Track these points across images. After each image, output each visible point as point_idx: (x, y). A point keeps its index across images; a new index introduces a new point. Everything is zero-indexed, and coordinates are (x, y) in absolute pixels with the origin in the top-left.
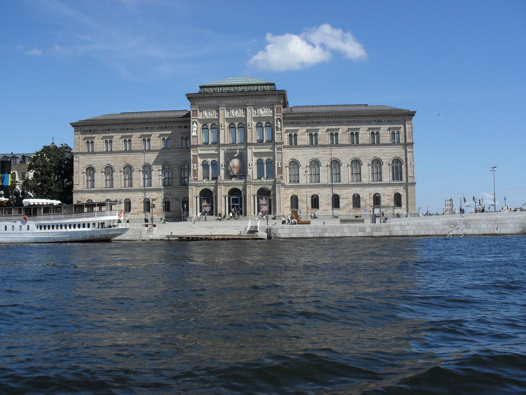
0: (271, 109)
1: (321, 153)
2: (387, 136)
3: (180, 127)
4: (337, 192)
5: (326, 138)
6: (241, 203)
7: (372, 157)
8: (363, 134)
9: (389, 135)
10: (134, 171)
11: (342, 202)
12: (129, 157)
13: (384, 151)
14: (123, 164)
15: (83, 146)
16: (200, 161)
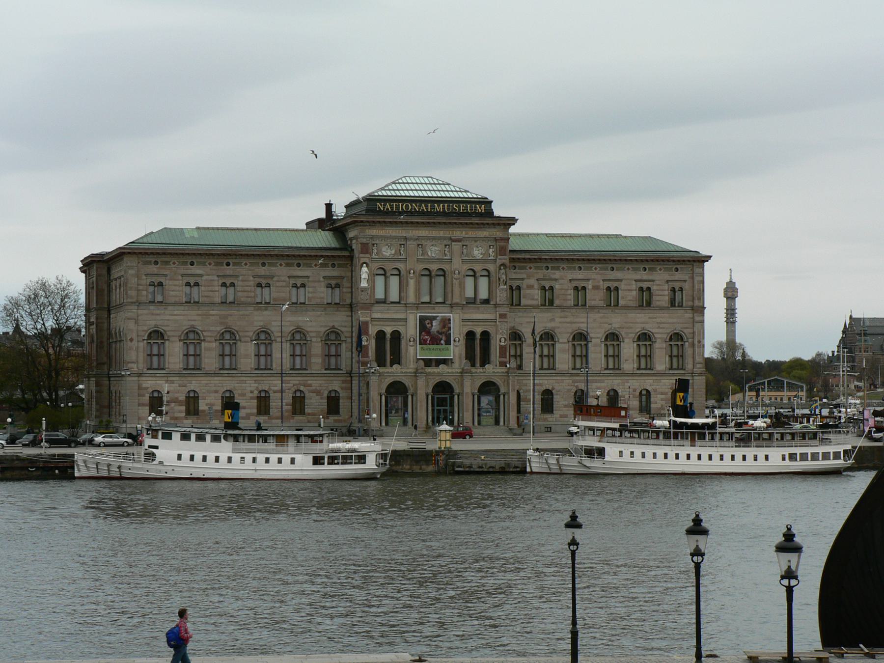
0: (490, 246)
1: (558, 320)
2: (664, 295)
5: (566, 295)
6: (452, 405)
7: (638, 329)
8: (624, 290)
9: (666, 293)
10: (240, 340)
12: (231, 316)
13: (658, 320)
14: (218, 329)
15: (143, 290)
16: (373, 330)
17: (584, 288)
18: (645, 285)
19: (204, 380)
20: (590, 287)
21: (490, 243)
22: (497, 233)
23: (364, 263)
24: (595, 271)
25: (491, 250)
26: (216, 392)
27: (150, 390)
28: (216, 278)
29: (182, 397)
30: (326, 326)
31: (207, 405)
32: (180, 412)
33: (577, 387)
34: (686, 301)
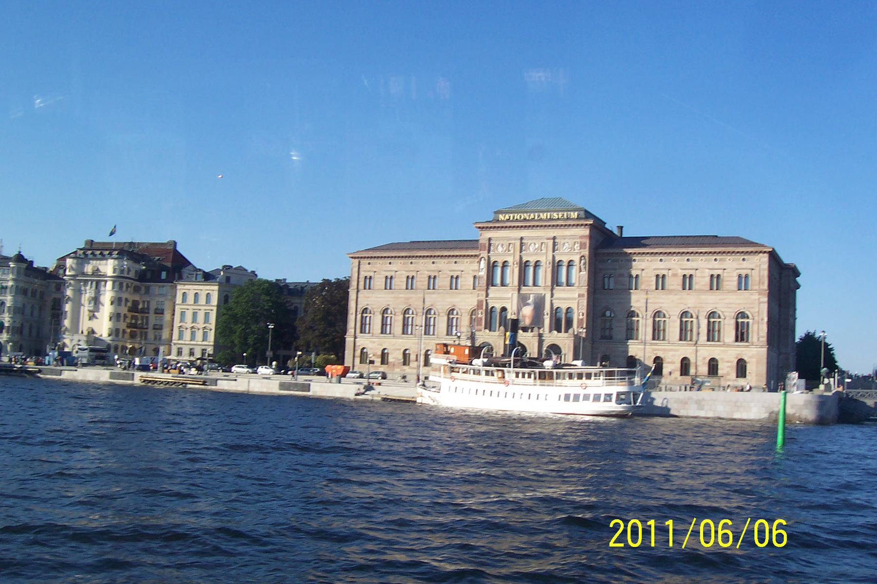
2: (733, 281)
4: (660, 354)
7: (709, 308)
13: (727, 301)
17: (664, 276)
18: (715, 273)
19: (394, 341)
20: (670, 274)
21: (575, 240)
23: (482, 258)
24: (673, 262)
25: (576, 245)
28: (404, 272)
29: (380, 353)
30: (471, 305)
31: (393, 358)
33: (656, 354)
34: (752, 285)
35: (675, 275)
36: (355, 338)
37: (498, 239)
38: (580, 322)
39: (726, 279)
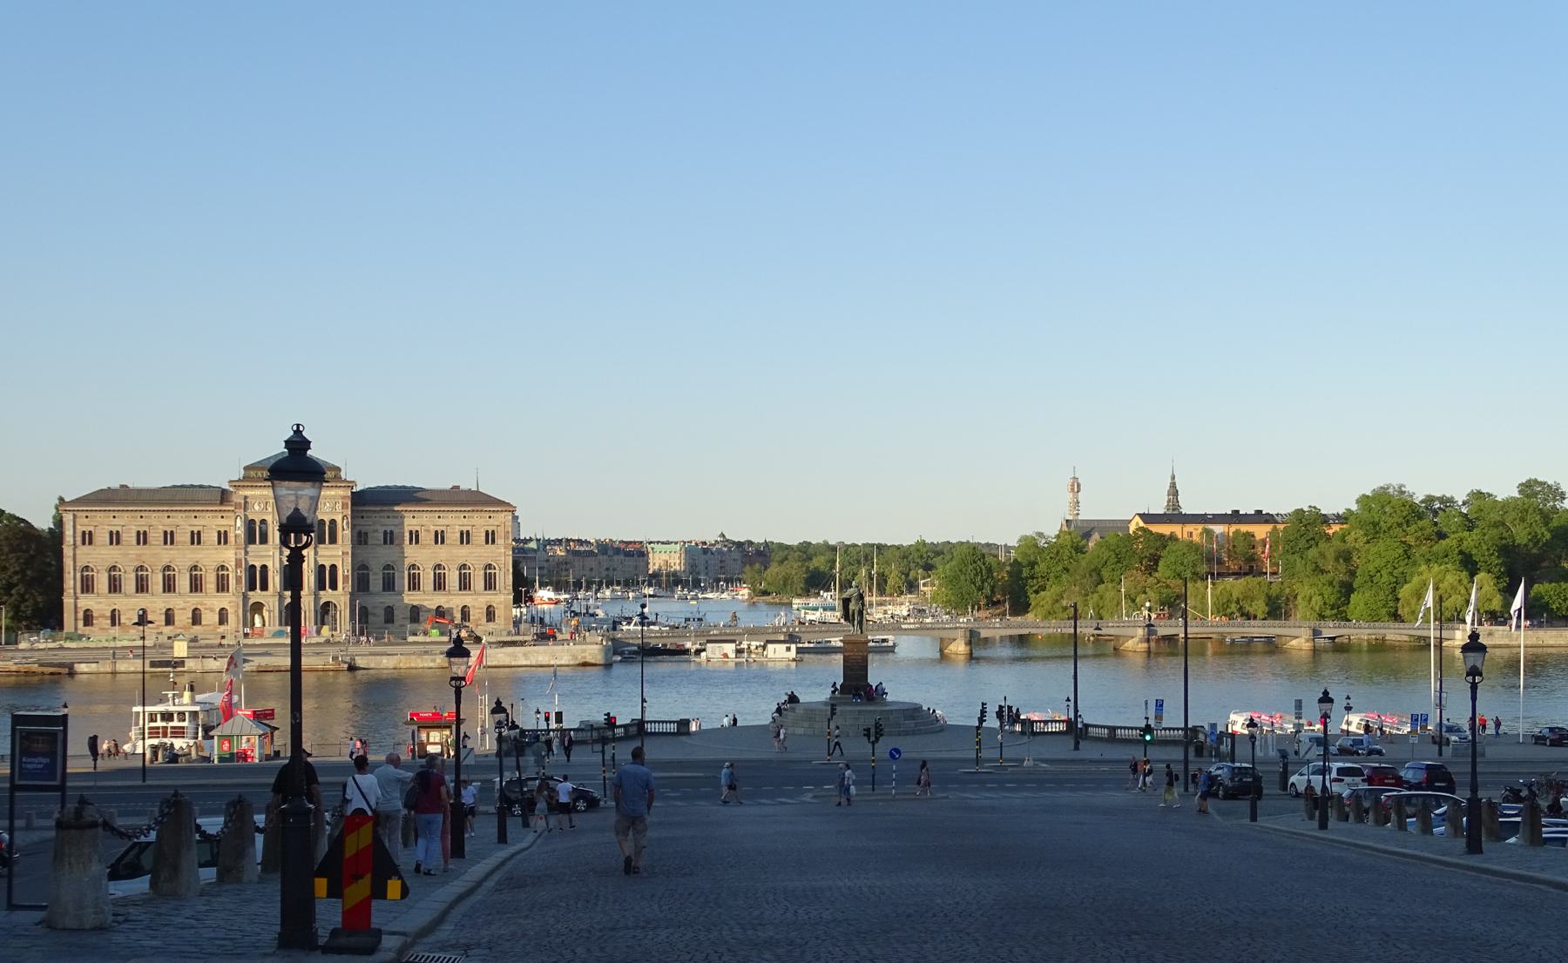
3: (217, 517)
7: (461, 562)
11: (423, 616)
13: (476, 554)
18: (465, 529)
19: (126, 600)
22: (341, 492)
26: (134, 610)
27: (84, 609)
28: (133, 527)
29: (109, 614)
31: (127, 619)
32: (108, 624)
35: (428, 531)
36: (76, 598)
37: (255, 497)
38: (345, 578)
39: (474, 534)
